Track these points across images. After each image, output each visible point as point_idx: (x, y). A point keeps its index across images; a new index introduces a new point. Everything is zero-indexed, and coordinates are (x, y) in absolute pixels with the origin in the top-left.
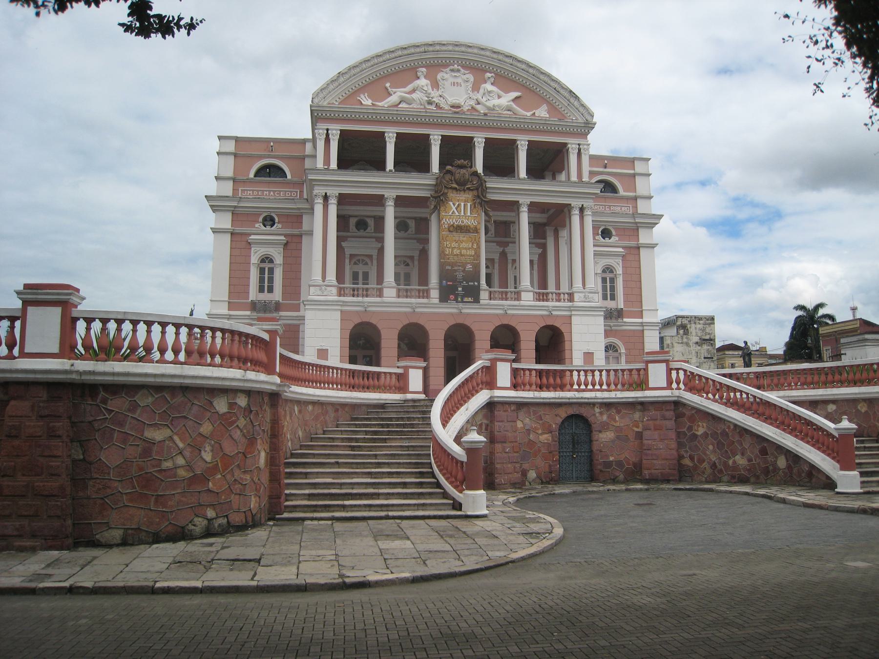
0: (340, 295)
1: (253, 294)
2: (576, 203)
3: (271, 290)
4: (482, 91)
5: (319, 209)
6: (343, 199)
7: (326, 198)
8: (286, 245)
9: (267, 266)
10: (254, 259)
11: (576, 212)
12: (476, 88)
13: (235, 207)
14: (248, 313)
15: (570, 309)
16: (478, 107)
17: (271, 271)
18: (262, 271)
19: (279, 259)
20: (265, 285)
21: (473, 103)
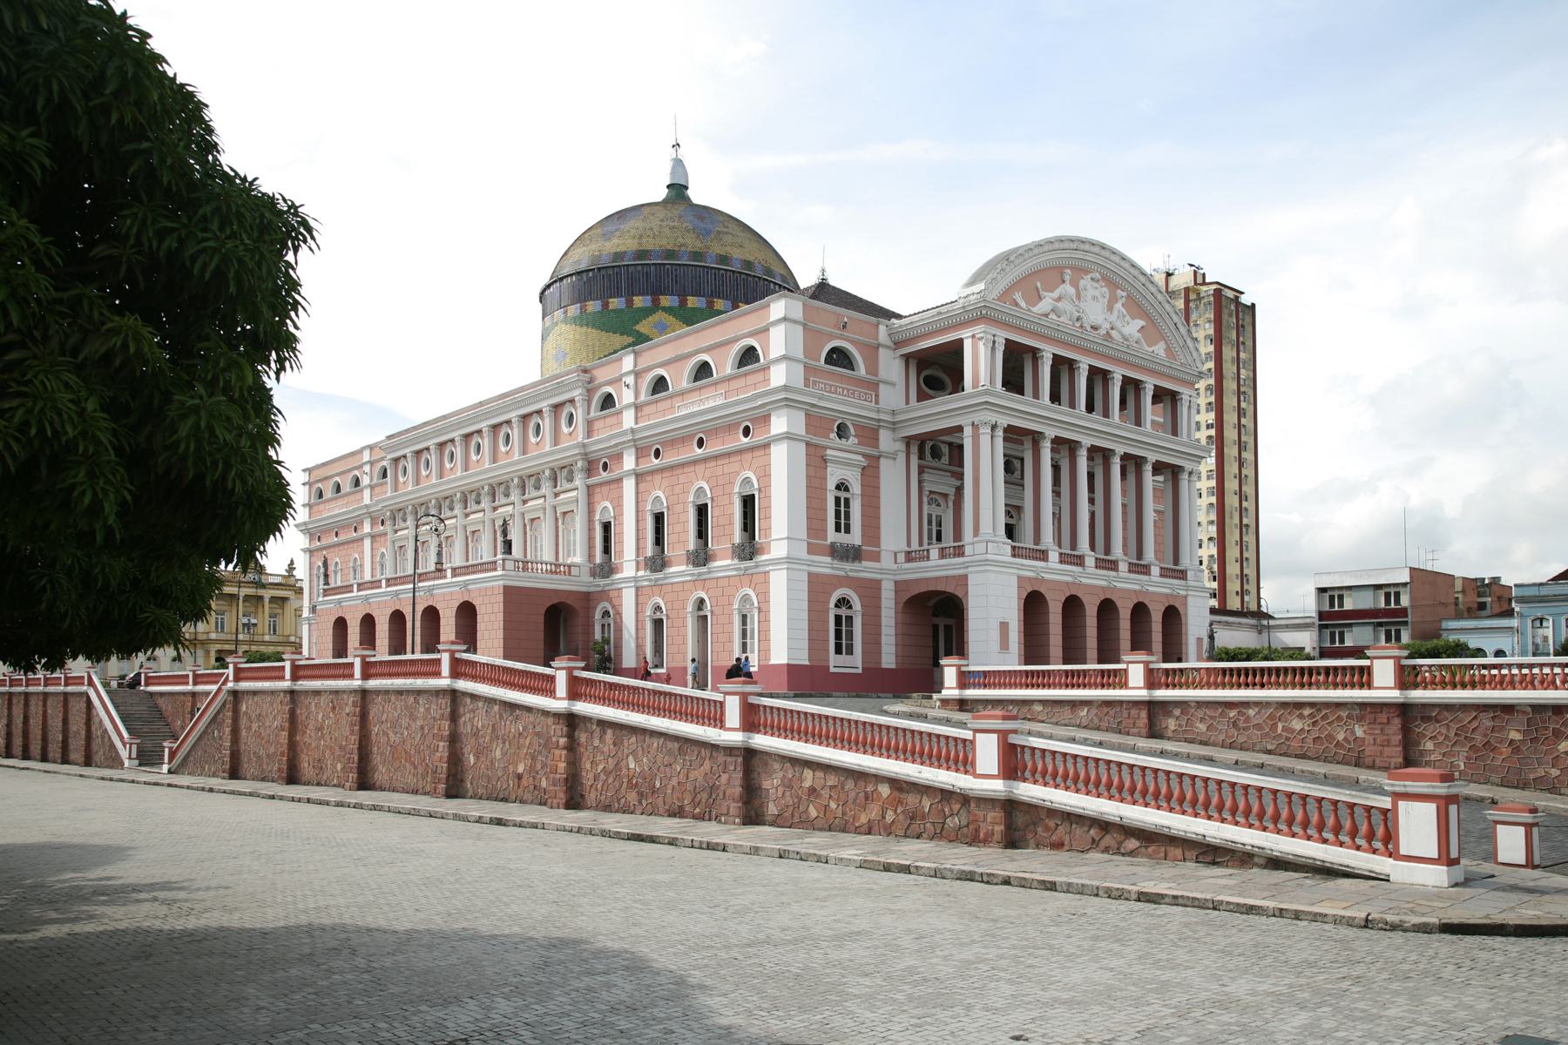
0: (1014, 556)
1: (832, 536)
2: (1188, 465)
3: (848, 531)
4: (1115, 312)
5: (985, 440)
6: (1009, 430)
7: (994, 427)
8: (864, 468)
9: (843, 495)
10: (831, 485)
11: (1185, 476)
12: (1110, 308)
13: (813, 405)
14: (828, 559)
15: (1187, 588)
16: (1114, 333)
17: (847, 501)
18: (837, 500)
19: (856, 488)
20: (843, 525)
21: (1108, 326)
